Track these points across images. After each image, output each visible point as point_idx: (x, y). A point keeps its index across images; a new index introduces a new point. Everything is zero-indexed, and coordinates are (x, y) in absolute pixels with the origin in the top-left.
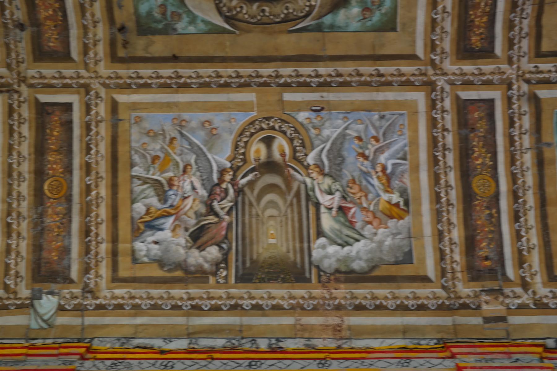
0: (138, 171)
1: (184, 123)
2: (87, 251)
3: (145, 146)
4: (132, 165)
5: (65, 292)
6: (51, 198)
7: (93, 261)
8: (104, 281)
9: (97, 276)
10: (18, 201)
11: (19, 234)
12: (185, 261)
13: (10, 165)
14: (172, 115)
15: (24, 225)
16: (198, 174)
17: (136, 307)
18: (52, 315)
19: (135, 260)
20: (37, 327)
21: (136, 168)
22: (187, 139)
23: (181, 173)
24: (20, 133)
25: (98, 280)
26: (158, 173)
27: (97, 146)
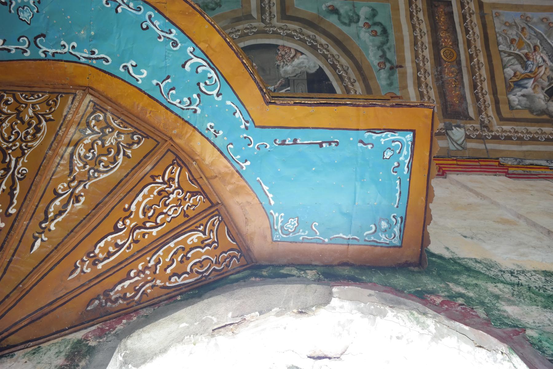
0: (502, 47)
1: (528, 19)
2: (478, 99)
3: (506, 32)
4: (498, 44)
5: (468, 126)
6: (446, 61)
7: (483, 106)
8: (494, 119)
9: (488, 116)
10: (423, 62)
11: (427, 85)
12: (547, 109)
13: (415, 37)
14: (520, 13)
15: (430, 79)
16: (544, 51)
17: (520, 139)
18: (463, 141)
19: (511, 108)
20: (455, 149)
21: (501, 46)
22: (532, 29)
23: (533, 51)
24: (418, 18)
25: (490, 119)
26: (518, 50)
27: (473, 29)
